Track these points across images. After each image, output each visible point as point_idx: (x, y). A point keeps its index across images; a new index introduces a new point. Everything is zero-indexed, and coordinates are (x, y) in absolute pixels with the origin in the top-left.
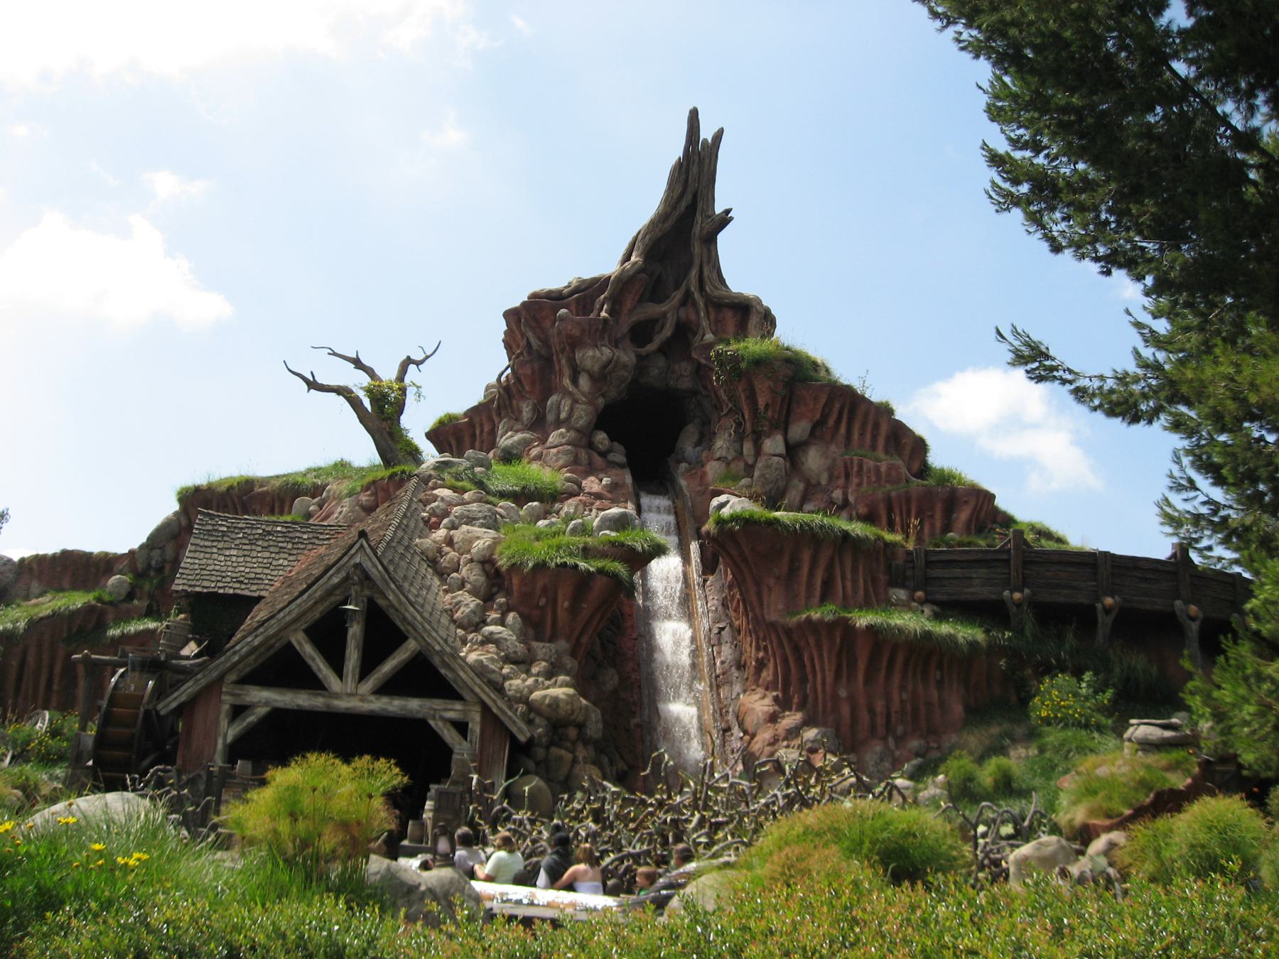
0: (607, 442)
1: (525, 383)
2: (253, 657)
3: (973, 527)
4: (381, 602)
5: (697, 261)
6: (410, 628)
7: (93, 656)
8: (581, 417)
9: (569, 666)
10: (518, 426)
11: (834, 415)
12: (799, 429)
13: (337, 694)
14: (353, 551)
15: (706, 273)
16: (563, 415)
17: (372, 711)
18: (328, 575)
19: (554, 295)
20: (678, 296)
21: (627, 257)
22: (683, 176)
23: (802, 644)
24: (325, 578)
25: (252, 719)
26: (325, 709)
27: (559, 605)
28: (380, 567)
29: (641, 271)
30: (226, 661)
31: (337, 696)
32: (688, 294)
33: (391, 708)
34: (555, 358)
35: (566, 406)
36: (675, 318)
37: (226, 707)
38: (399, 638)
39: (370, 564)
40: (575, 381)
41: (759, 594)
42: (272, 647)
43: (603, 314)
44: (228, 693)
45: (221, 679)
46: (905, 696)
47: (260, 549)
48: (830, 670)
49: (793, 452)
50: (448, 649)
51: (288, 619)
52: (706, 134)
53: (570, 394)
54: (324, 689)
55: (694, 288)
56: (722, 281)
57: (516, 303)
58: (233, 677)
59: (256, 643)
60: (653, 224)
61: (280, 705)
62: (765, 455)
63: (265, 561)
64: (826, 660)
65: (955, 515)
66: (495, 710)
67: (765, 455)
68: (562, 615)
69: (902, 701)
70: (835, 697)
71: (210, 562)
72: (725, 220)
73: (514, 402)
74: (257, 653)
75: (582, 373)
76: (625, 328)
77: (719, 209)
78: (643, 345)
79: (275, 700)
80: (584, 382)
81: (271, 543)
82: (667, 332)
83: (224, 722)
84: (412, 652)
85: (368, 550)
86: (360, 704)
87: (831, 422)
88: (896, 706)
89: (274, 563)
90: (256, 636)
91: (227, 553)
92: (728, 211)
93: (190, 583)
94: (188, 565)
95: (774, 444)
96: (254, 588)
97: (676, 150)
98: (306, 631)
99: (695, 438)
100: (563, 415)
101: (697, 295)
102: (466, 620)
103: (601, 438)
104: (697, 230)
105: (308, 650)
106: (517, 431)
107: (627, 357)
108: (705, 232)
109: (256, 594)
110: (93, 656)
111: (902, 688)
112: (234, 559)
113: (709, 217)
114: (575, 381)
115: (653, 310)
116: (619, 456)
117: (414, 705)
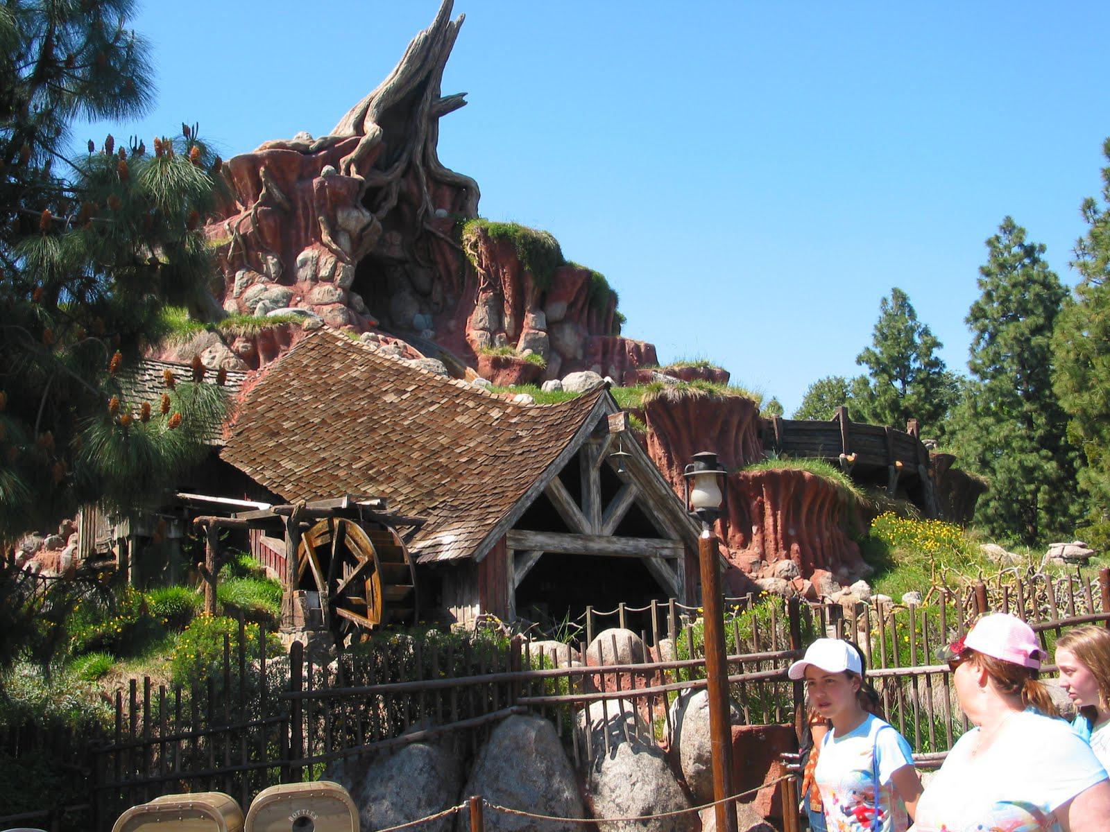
17: (616, 552)
20: (400, 167)
25: (531, 563)
33: (628, 549)
37: (511, 553)
52: (454, 18)
54: (580, 532)
61: (551, 549)
77: (447, 88)
79: (548, 545)
82: (393, 202)
83: (511, 568)
85: (610, 400)
86: (608, 545)
92: (464, 94)
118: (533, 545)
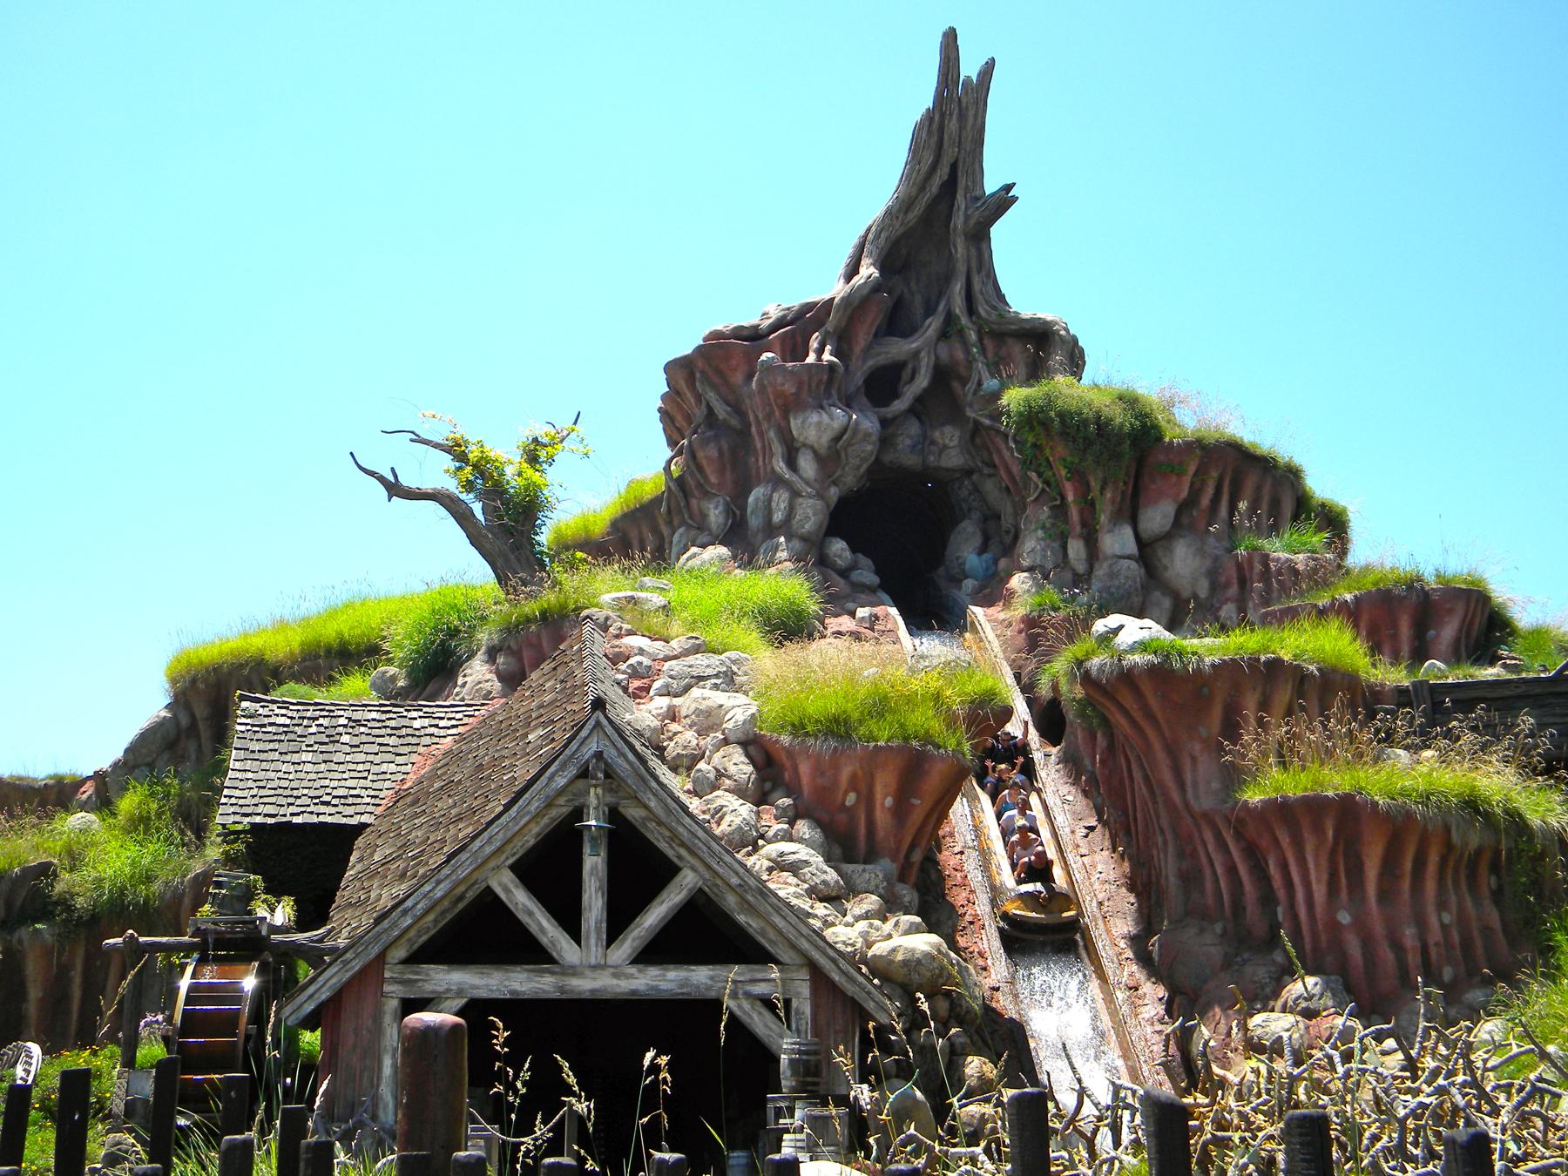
0: (848, 554)
1: (708, 471)
2: (431, 917)
3: (1463, 648)
4: (633, 813)
5: (961, 268)
6: (683, 852)
7: (142, 939)
8: (807, 518)
9: (907, 899)
10: (703, 538)
11: (1209, 492)
12: (1157, 517)
13: (572, 967)
14: (584, 733)
15: (977, 286)
16: (778, 517)
17: (634, 992)
18: (548, 774)
19: (745, 333)
20: (933, 325)
21: (852, 270)
22: (935, 138)
23: (1264, 842)
24: (544, 779)
26: (557, 995)
27: (878, 803)
28: (630, 756)
29: (875, 288)
30: (391, 928)
31: (573, 971)
32: (950, 318)
33: (664, 985)
34: (753, 429)
35: (781, 500)
36: (933, 358)
38: (666, 871)
39: (614, 752)
40: (792, 464)
41: (1177, 771)
42: (461, 897)
43: (827, 356)
44: (394, 981)
45: (381, 958)
46: (1447, 918)
47: (348, 749)
48: (1319, 881)
49: (1147, 551)
50: (752, 882)
51: (488, 850)
52: (969, 69)
53: (787, 485)
54: (552, 961)
55: (959, 306)
56: (1002, 298)
57: (686, 348)
58: (400, 953)
59: (439, 893)
60: (889, 213)
62: (1106, 559)
63: (360, 767)
64: (1311, 865)
65: (1432, 633)
66: (836, 977)
67: (1106, 559)
68: (882, 818)
69: (1443, 927)
70: (1334, 925)
71: (272, 775)
72: (1004, 201)
73: (694, 502)
74: (438, 909)
75: (803, 450)
76: (859, 378)
77: (991, 185)
78: (886, 403)
80: (807, 465)
81: (364, 738)
82: (923, 381)
84: (690, 890)
85: (609, 729)
86: (615, 982)
87: (1205, 501)
88: (1435, 935)
89: (375, 769)
90: (439, 882)
91: (295, 758)
92: (1009, 187)
93: (245, 810)
94: (236, 783)
95: (1118, 541)
96: (350, 810)
97: (923, 97)
98: (512, 868)
99: (977, 541)
100: (778, 517)
101: (964, 320)
102: (737, 837)
103: (838, 548)
104: (958, 221)
105: (520, 900)
106: (704, 546)
107: (867, 423)
108: (972, 222)
109: (354, 821)
110: (142, 939)
111: (1442, 906)
112: (309, 767)
113: (977, 199)
114: (792, 464)
115: (898, 348)
116: (868, 575)
117: (700, 978)
118: (441, 989)
